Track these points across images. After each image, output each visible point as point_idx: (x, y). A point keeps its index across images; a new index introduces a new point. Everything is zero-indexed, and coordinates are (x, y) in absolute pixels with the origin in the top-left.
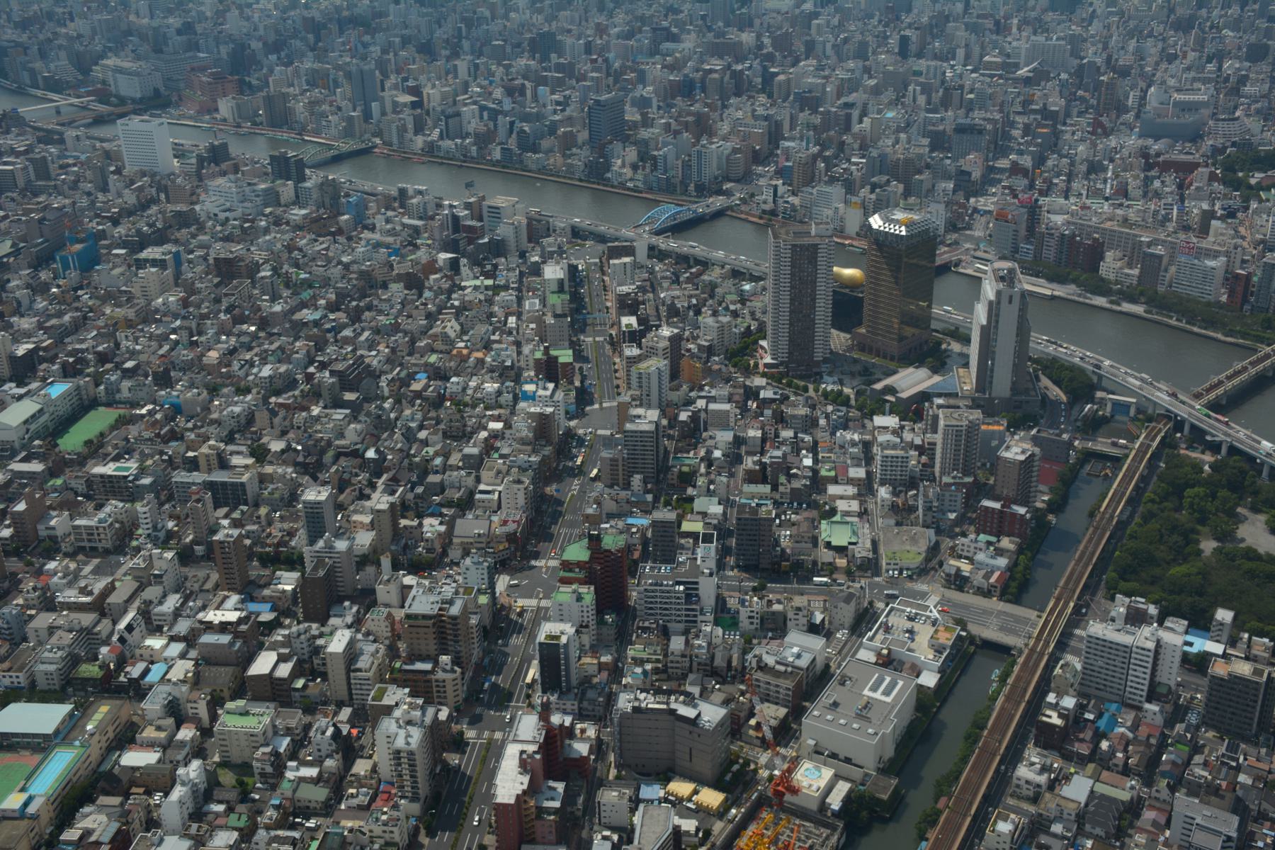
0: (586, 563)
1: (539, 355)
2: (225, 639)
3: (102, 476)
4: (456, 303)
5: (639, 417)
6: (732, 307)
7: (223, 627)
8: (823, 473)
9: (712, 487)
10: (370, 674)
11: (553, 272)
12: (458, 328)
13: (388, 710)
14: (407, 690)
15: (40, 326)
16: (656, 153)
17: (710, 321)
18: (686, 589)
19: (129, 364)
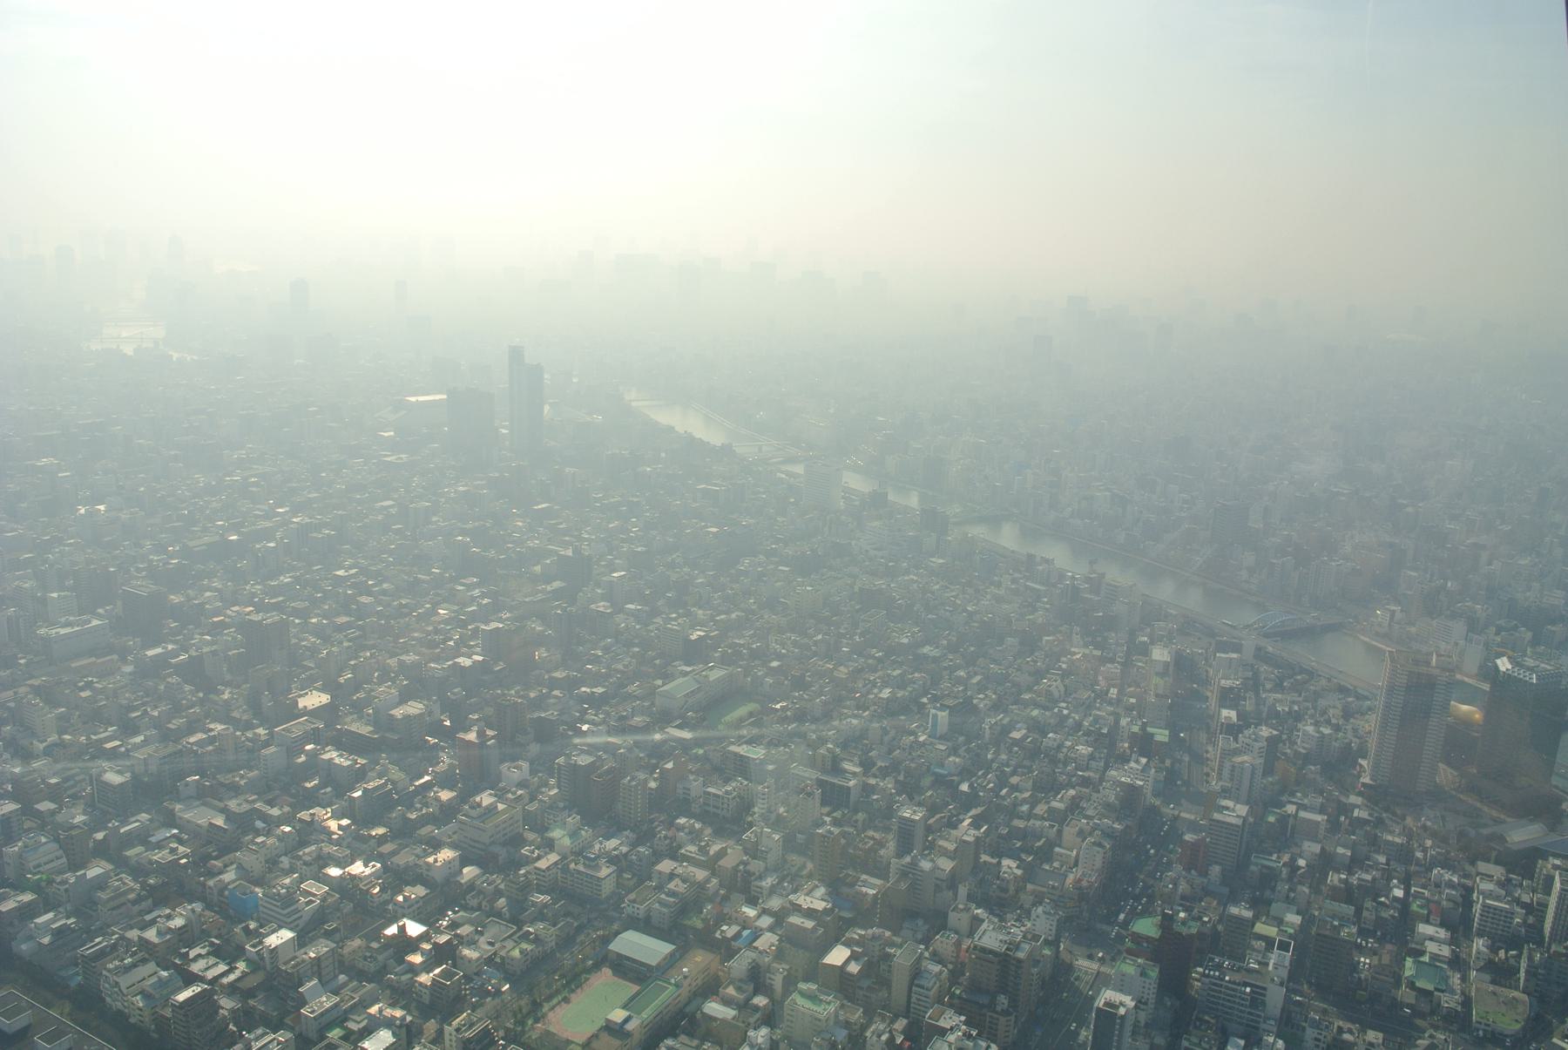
0: (1156, 940)
1: (1136, 729)
2: (809, 924)
3: (736, 754)
4: (1064, 666)
5: (1227, 808)
6: (1334, 721)
7: (810, 913)
8: (1414, 907)
9: (1292, 895)
10: (932, 993)
11: (1160, 654)
12: (1062, 689)
13: (943, 1032)
14: (963, 1018)
15: (712, 618)
16: (1275, 561)
17: (1310, 729)
18: (1252, 991)
19: (775, 664)
